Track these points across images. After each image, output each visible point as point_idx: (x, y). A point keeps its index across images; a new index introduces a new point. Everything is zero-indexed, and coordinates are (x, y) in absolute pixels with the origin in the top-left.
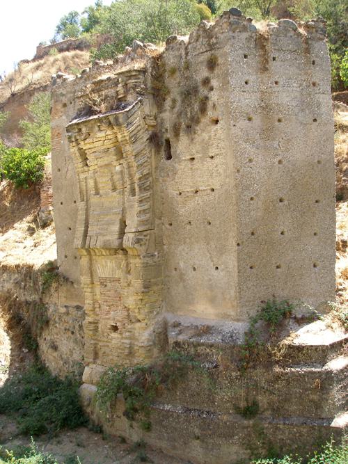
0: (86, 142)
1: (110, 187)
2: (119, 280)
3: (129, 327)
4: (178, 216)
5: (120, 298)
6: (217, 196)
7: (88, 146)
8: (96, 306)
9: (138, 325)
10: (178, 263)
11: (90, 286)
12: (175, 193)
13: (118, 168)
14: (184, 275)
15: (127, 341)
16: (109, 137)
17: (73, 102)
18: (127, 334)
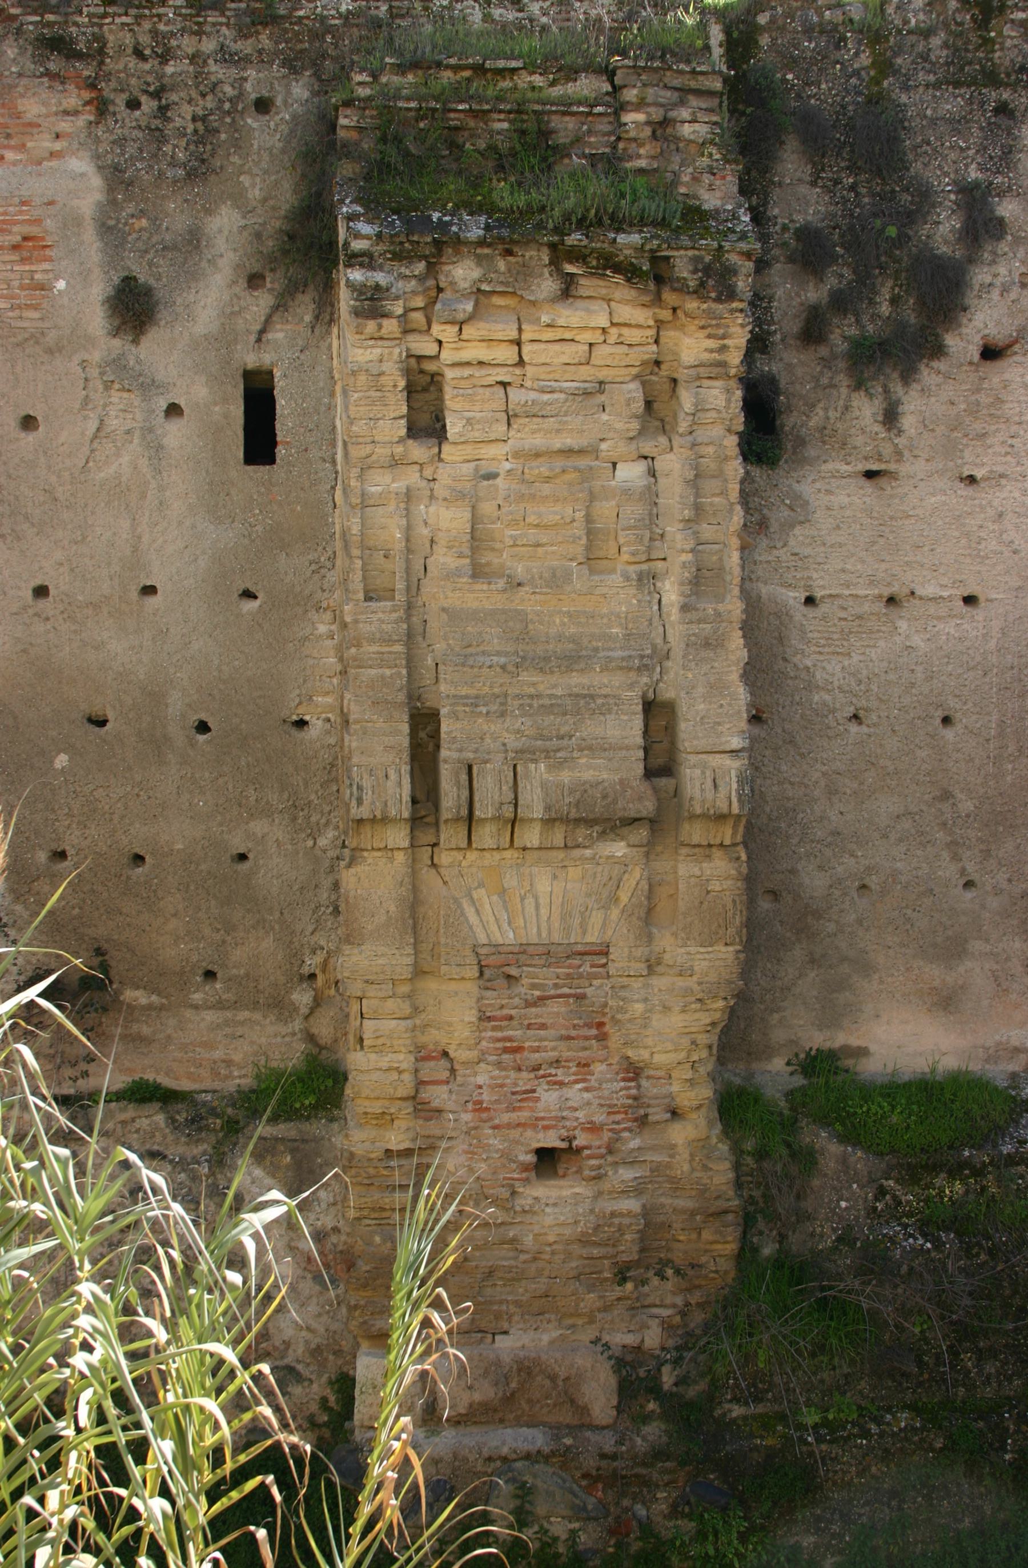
0: (468, 331)
1: (578, 550)
2: (604, 951)
3: (635, 1143)
4: (811, 686)
5: (600, 1025)
6: (996, 625)
7: (466, 355)
8: (424, 1075)
9: (680, 1134)
10: (793, 871)
11: (404, 989)
12: (794, 597)
13: (631, 473)
14: (818, 915)
15: (632, 1205)
16: (633, 335)
17: (148, 105)
18: (627, 1174)
